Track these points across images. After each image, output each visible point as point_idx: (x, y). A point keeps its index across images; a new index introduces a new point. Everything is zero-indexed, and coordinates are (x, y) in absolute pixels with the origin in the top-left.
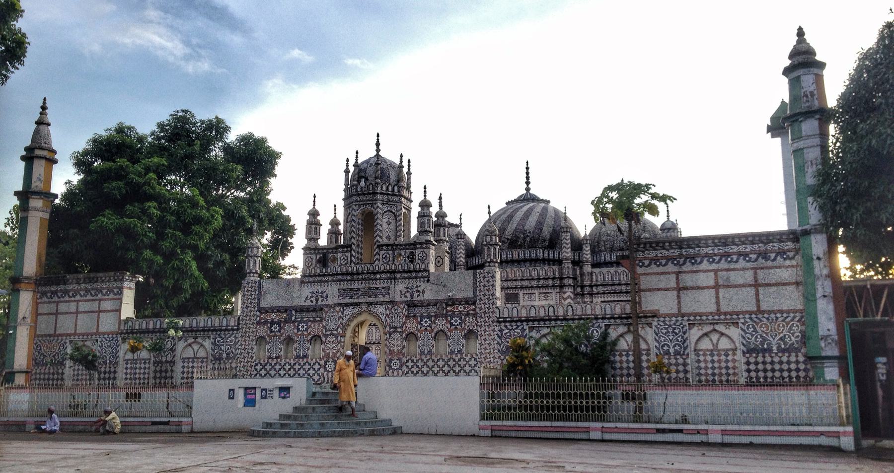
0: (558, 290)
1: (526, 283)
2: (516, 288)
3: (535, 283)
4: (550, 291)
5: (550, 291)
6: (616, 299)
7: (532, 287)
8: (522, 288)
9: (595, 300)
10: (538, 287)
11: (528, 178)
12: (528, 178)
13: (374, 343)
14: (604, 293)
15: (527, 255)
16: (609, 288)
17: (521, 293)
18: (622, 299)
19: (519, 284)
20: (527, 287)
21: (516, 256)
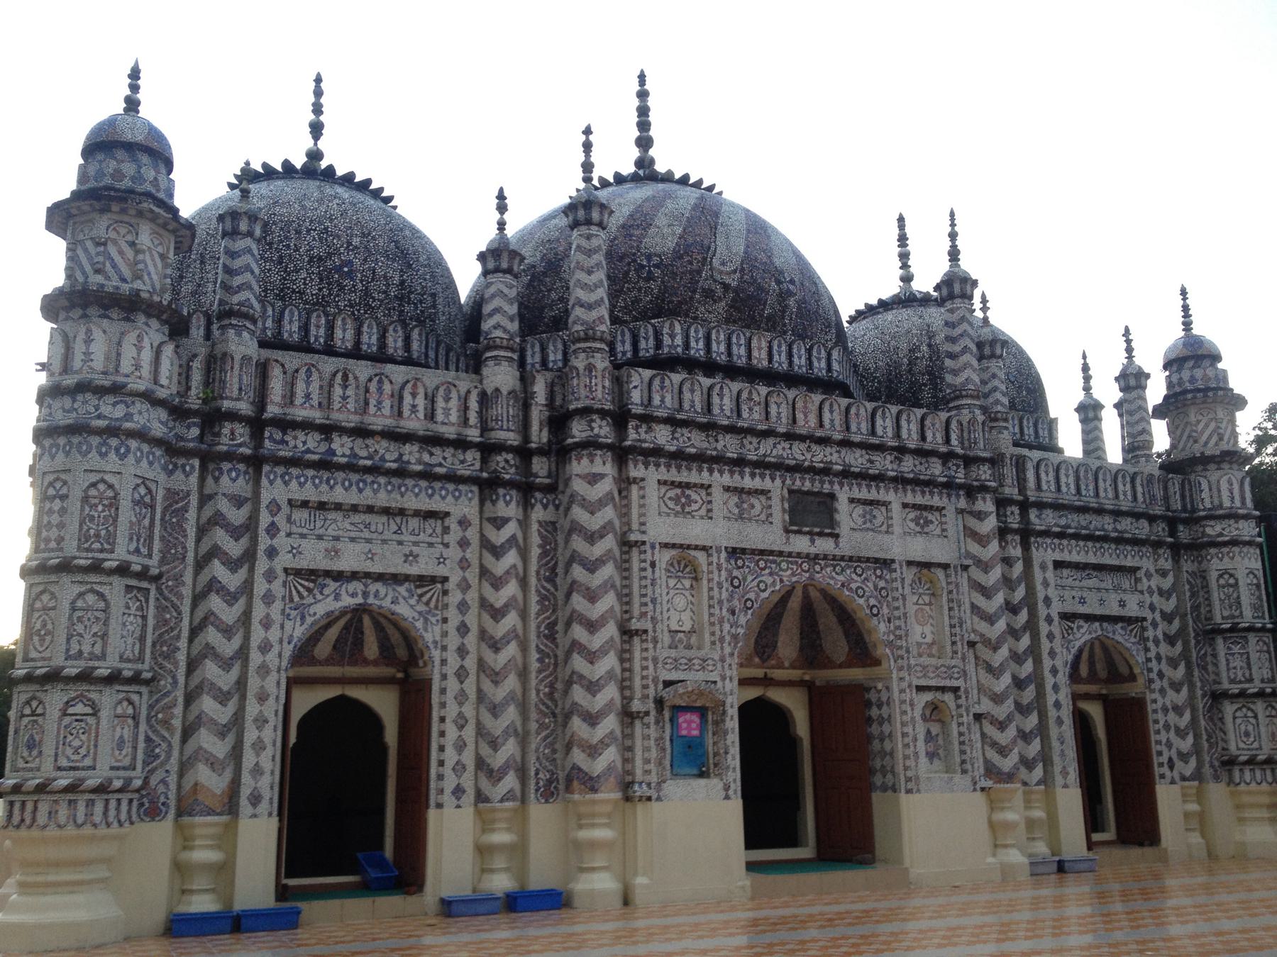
0: (962, 503)
1: (857, 460)
2: (826, 471)
3: (884, 463)
4: (936, 501)
5: (936, 501)
6: (1092, 559)
7: (879, 478)
8: (846, 474)
9: (1037, 555)
10: (901, 481)
11: (644, 125)
12: (644, 125)
13: (113, 678)
14: (1061, 535)
15: (800, 361)
16: (1074, 521)
17: (843, 495)
18: (1107, 560)
19: (834, 457)
20: (863, 476)
21: (760, 359)
